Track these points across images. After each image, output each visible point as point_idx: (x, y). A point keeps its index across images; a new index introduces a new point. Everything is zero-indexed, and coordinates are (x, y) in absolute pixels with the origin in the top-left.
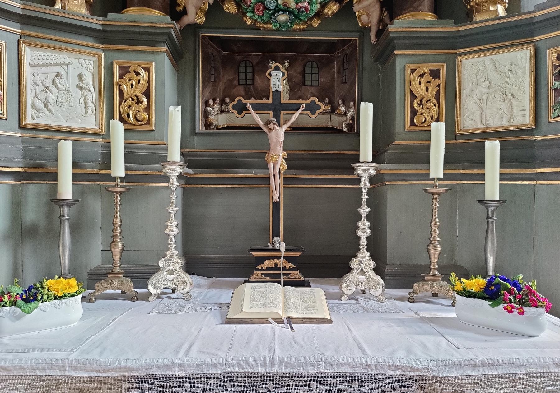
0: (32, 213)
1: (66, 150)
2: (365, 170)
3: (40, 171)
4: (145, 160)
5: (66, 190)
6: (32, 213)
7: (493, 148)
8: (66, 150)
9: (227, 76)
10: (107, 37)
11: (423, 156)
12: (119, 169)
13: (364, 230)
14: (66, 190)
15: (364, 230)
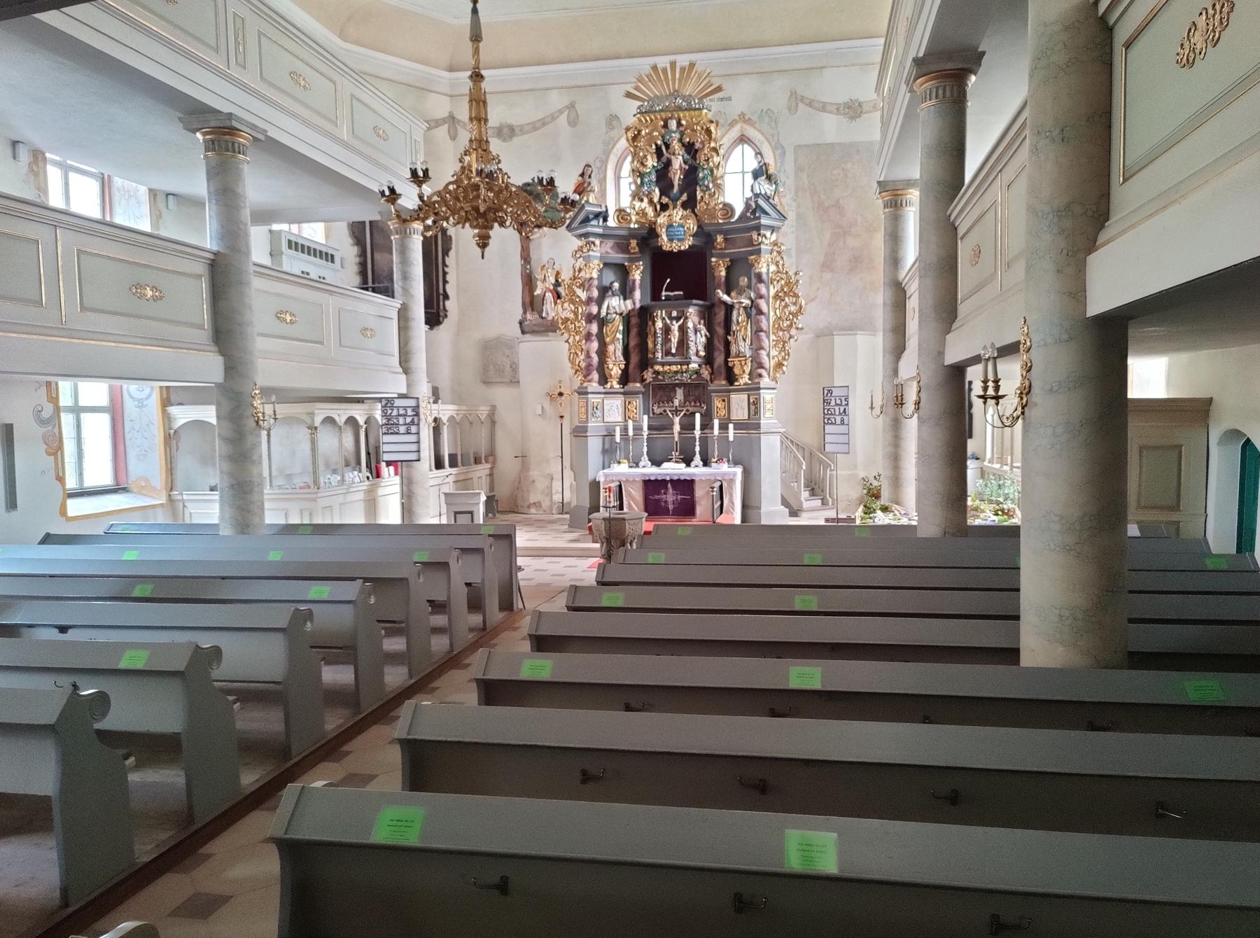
0: (607, 446)
1: (618, 430)
2: (697, 432)
3: (611, 434)
4: (638, 429)
5: (618, 439)
6: (607, 446)
7: (731, 426)
8: (618, 430)
9: (660, 393)
10: (624, 393)
11: (712, 428)
12: (631, 433)
13: (697, 449)
14: (618, 439)
15: (697, 449)
